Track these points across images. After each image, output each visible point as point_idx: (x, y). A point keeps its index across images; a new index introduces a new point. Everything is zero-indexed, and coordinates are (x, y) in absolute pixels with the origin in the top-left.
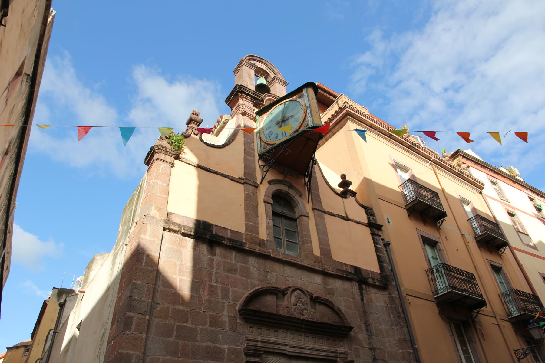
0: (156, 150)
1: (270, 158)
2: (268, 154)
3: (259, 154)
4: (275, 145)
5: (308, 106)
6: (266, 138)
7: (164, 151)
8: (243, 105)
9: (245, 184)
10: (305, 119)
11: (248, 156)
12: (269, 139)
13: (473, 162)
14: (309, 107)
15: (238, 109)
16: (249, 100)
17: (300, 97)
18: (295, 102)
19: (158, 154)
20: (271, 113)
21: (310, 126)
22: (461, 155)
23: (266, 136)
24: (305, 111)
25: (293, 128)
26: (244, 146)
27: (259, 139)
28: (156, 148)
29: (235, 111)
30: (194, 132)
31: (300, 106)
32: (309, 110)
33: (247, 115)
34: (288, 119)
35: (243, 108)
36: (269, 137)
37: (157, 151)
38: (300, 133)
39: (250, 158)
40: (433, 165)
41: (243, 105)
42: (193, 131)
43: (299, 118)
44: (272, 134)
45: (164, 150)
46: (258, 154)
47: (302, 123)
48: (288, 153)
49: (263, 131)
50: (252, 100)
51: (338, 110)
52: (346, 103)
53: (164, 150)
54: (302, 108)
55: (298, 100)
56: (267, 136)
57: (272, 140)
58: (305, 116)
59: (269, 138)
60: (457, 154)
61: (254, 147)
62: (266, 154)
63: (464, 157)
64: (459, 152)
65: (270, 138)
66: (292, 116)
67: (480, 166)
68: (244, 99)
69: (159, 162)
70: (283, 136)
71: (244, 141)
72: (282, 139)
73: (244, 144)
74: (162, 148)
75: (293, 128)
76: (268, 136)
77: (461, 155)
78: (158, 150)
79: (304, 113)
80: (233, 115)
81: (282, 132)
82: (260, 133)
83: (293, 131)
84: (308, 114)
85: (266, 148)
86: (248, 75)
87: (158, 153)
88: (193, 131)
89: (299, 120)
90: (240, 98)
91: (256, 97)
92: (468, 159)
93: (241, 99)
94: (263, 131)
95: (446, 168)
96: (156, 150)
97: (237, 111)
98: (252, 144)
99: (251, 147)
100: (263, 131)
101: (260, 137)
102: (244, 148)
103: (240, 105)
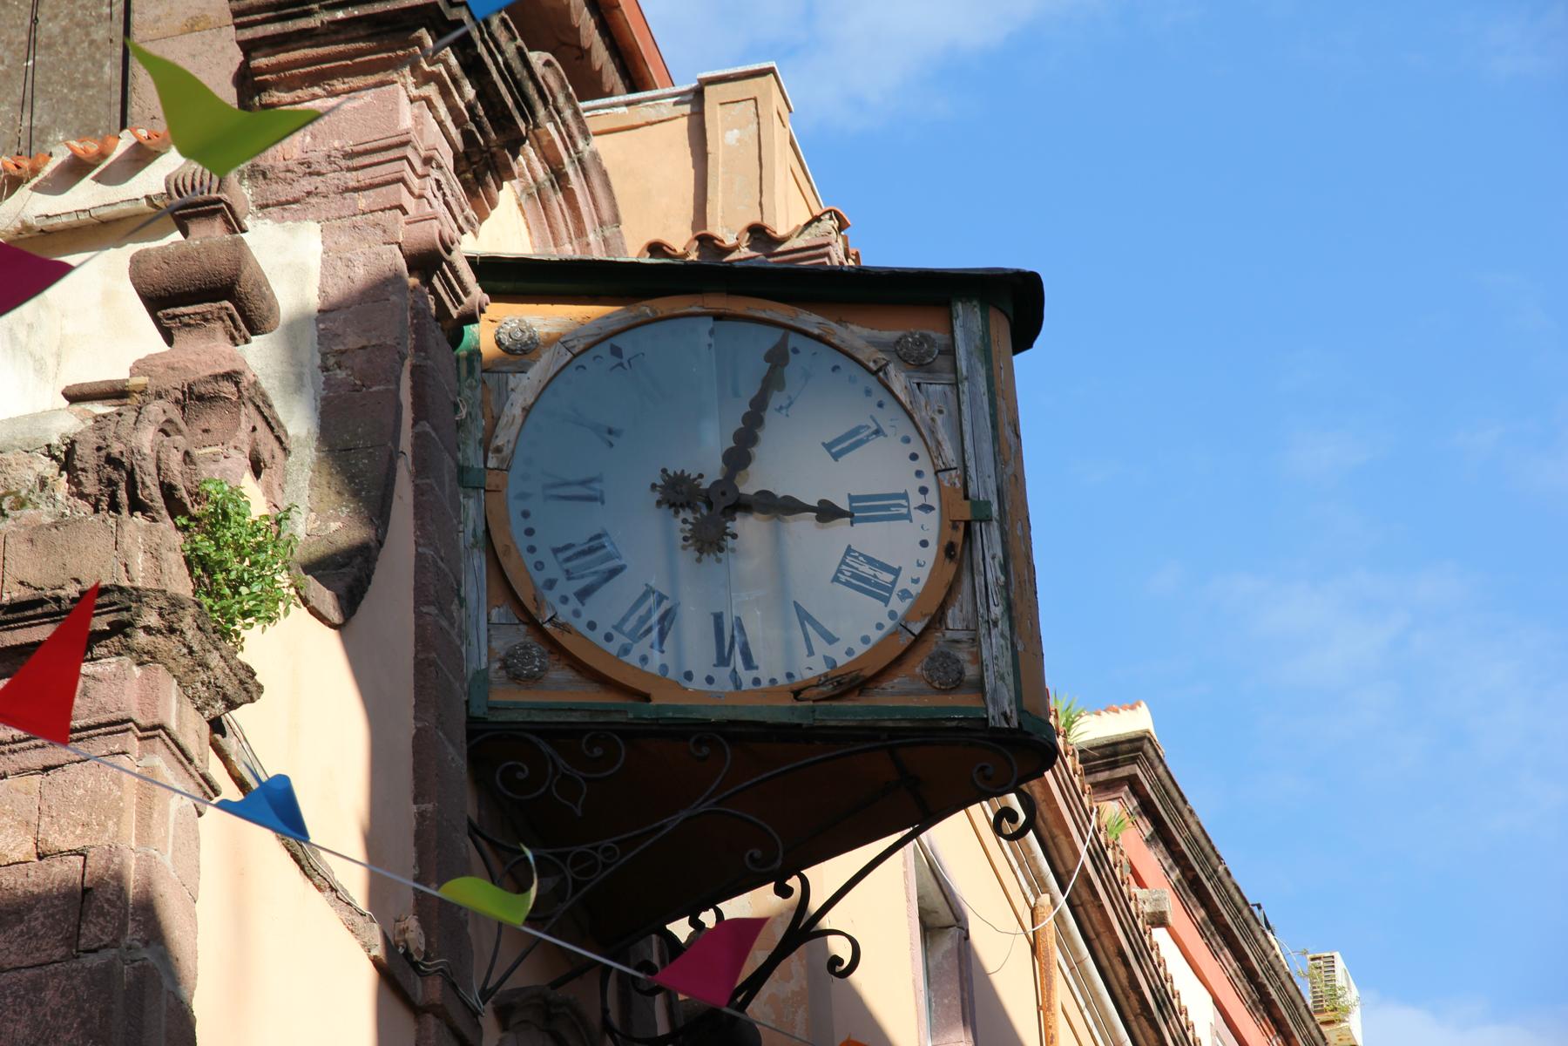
0: (148, 630)
1: (579, 812)
2: (561, 762)
3: (478, 712)
4: (646, 712)
5: (988, 504)
6: (550, 584)
7: (187, 661)
8: (427, 161)
9: (431, 1020)
10: (943, 608)
11: (445, 734)
12: (574, 603)
13: (1176, 874)
14: (995, 524)
15: (364, 176)
16: (453, 109)
17: (918, 361)
18: (868, 392)
19: (140, 664)
20: (616, 352)
21: (997, 722)
22: (1133, 783)
23: (543, 554)
24: (958, 537)
25: (831, 639)
26: (419, 615)
27: (479, 560)
28: (152, 619)
29: (324, 167)
30: (261, 448)
32: (1000, 554)
33: (435, 280)
35: (415, 182)
36: (579, 584)
37: (141, 638)
38: (894, 732)
40: (1045, 898)
41: (427, 161)
42: (254, 429)
43: (896, 572)
44: (614, 572)
45: (196, 648)
47: (919, 639)
48: (757, 853)
50: (474, 116)
51: (729, 241)
52: (829, 224)
53: (191, 652)
55: (899, 380)
56: (553, 569)
58: (952, 589)
59: (583, 594)
60: (1113, 765)
62: (546, 748)
63: (1147, 808)
64: (1133, 760)
65: (591, 601)
66: (827, 512)
67: (1201, 914)
68: (431, 90)
69: (161, 762)
70: (723, 660)
74: (189, 634)
76: (569, 575)
77: (1133, 783)
78: (160, 639)
80: (284, 192)
81: (718, 618)
82: (485, 491)
83: (821, 668)
85: (533, 679)
87: (145, 658)
88: (254, 429)
89: (890, 591)
90: (407, 70)
91: (509, 101)
92: (1162, 835)
93: (410, 80)
95: (1097, 945)
96: (148, 630)
97: (352, 179)
101: (487, 531)
103: (409, 152)
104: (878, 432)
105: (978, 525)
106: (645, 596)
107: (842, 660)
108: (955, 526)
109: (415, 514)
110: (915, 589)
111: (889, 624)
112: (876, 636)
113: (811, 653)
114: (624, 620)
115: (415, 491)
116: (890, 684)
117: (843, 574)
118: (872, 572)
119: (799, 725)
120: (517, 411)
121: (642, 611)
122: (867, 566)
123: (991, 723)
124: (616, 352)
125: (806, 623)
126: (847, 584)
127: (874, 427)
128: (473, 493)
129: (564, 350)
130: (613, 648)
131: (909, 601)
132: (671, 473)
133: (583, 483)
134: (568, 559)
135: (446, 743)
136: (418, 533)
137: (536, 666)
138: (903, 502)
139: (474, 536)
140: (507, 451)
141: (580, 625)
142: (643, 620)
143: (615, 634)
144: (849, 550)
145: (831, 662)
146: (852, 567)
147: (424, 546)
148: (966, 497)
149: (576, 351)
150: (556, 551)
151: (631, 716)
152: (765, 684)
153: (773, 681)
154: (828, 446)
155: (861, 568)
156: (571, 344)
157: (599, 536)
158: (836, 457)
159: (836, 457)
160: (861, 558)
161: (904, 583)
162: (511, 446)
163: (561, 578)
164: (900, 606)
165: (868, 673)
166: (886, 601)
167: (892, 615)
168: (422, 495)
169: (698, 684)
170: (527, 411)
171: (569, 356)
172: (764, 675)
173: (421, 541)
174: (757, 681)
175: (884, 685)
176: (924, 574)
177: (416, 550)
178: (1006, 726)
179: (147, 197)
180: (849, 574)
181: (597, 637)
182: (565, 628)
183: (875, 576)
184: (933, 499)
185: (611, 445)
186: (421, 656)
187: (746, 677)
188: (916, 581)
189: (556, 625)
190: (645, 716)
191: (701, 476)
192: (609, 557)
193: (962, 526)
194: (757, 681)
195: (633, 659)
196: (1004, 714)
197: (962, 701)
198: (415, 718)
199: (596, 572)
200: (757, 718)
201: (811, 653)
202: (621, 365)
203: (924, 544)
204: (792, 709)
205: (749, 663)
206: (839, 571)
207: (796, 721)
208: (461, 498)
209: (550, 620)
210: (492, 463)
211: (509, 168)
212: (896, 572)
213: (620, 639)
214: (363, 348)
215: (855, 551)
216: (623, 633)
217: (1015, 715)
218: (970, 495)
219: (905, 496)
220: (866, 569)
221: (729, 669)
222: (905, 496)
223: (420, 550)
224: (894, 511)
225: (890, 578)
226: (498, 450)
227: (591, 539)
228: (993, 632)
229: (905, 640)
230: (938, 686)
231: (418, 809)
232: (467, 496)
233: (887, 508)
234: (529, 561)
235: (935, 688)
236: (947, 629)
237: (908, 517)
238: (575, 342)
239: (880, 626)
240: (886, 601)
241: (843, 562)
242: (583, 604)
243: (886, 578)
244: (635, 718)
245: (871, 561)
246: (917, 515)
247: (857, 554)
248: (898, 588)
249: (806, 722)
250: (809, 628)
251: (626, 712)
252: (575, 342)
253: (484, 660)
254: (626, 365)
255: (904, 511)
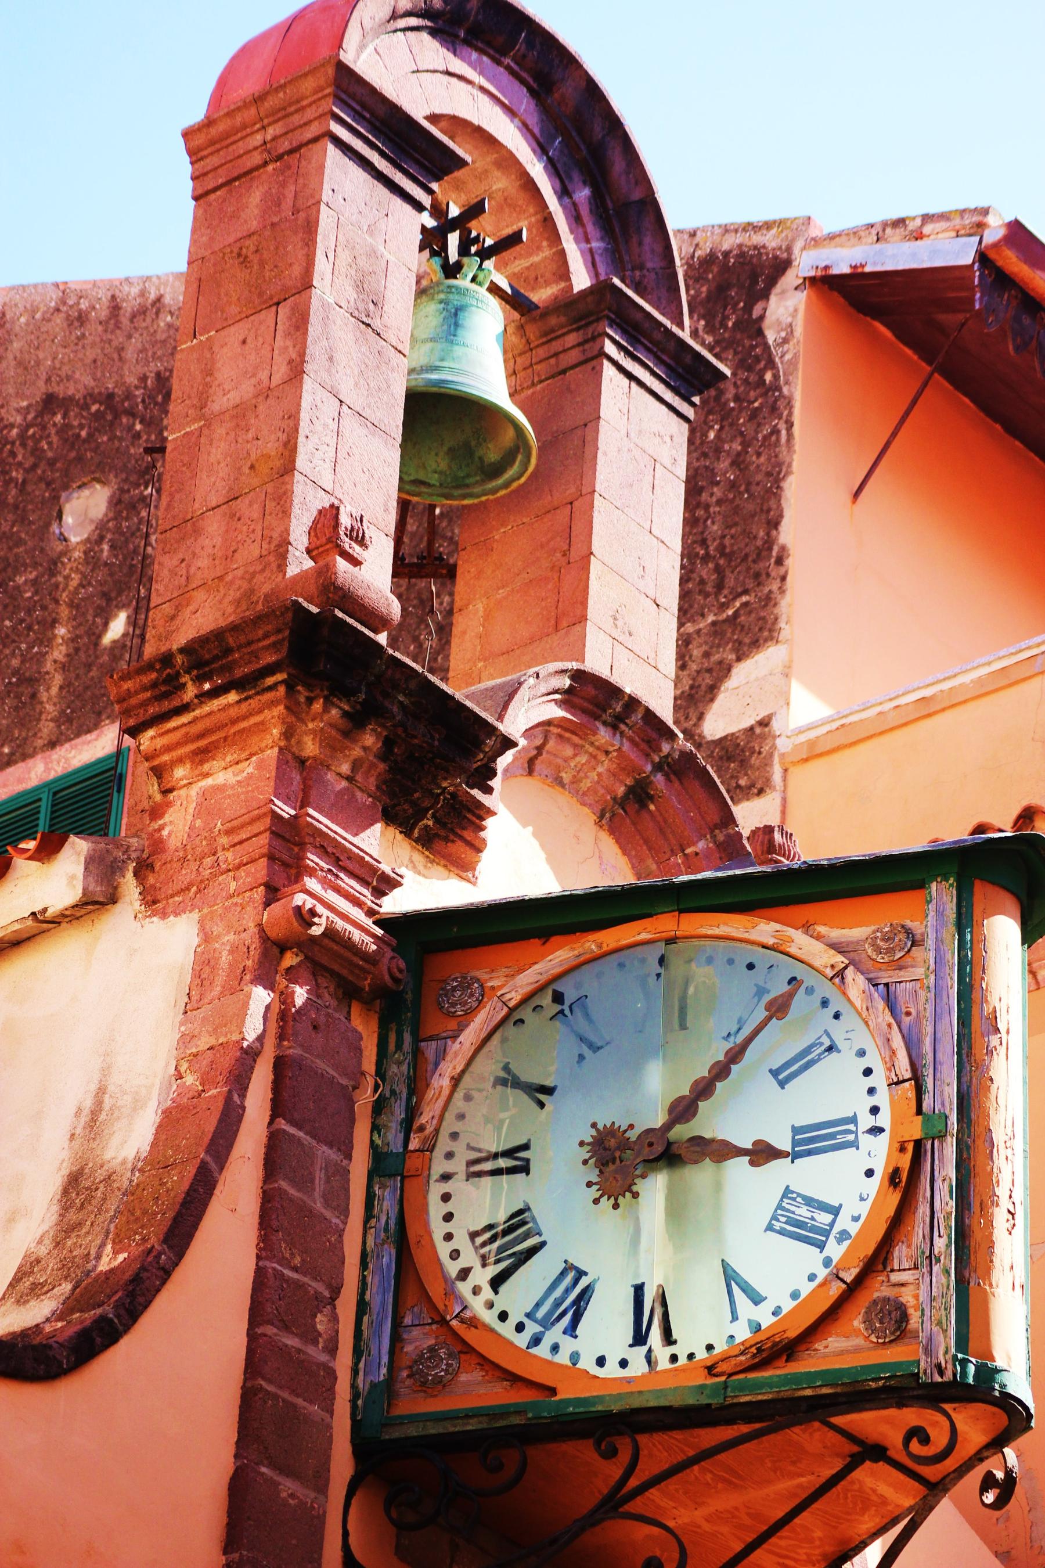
6: (464, 1274)
12: (487, 1292)
20: (558, 998)
23: (461, 1241)
25: (757, 1299)
27: (388, 1257)
31: (868, 1072)
34: (723, 1151)
39: (288, 1486)
43: (835, 1211)
46: (356, 1425)
49: (439, 1166)
54: (875, 1110)
56: (469, 1258)
57: (520, 1328)
59: (496, 1283)
61: (332, 1349)
70: (640, 1338)
71: (260, 1274)
72: (624, 1363)
73: (256, 1314)
75: (757, 1299)
79: (893, 1178)
81: (639, 1290)
82: (403, 1178)
83: (743, 1333)
84: (923, 1209)
86: (360, 286)
89: (827, 1233)
94: (446, 1177)
98: (321, 1322)
99: (311, 1350)
100: (446, 1177)
102: (252, 1366)
104: (830, 1049)
105: (930, 1142)
106: (563, 1274)
107: (767, 1320)
108: (902, 1149)
109: (260, 1224)
110: (854, 1229)
111: (822, 1273)
112: (806, 1289)
113: (735, 1318)
114: (538, 1305)
115: (263, 1199)
116: (824, 1343)
117: (778, 1220)
118: (809, 1215)
119: (709, 1405)
120: (446, 1082)
121: (558, 1293)
122: (805, 1208)
123: (923, 1379)
124: (558, 998)
125: (733, 1283)
126: (782, 1232)
127: (827, 1043)
128: (390, 1182)
129: (500, 1004)
130: (521, 1341)
131: (847, 1243)
132: (600, 1127)
133: (509, 1153)
134: (484, 1244)
135: (278, 1478)
136: (262, 1245)
137: (443, 1370)
138: (852, 1127)
139: (386, 1230)
140: (429, 1129)
141: (489, 1317)
142: (558, 1303)
143: (526, 1321)
144: (787, 1191)
145: (757, 1328)
146: (788, 1211)
147: (267, 1258)
148: (919, 1111)
149: (511, 1004)
150: (473, 1235)
151: (530, 1415)
152: (682, 1360)
153: (691, 1356)
154: (775, 1073)
155: (798, 1211)
156: (508, 996)
157: (520, 1212)
158: (782, 1084)
159: (782, 1084)
160: (799, 1199)
161: (844, 1222)
162: (435, 1122)
163: (477, 1264)
164: (835, 1250)
165: (792, 1334)
166: (821, 1246)
167: (827, 1261)
168: (269, 1202)
169: (611, 1370)
170: (456, 1081)
171: (506, 1009)
172: (681, 1350)
173: (264, 1254)
174: (674, 1358)
175: (816, 1346)
176: (864, 1209)
177: (257, 1265)
178: (940, 1380)
179: (33, 914)
180: (783, 1219)
181: (506, 1330)
182: (474, 1323)
183: (813, 1219)
184: (884, 1119)
185: (542, 1105)
186: (249, 1385)
187: (662, 1354)
188: (855, 1219)
189: (463, 1321)
190: (545, 1414)
191: (631, 1126)
192: (527, 1236)
193: (910, 1147)
194: (674, 1358)
195: (542, 1351)
196: (939, 1366)
197: (897, 1354)
198: (236, 1456)
199: (514, 1254)
200: (663, 1402)
201: (735, 1318)
202: (562, 1012)
203: (869, 1173)
204: (701, 1388)
205: (668, 1338)
206: (774, 1217)
207: (705, 1401)
208: (376, 1189)
209: (456, 1316)
210: (412, 1147)
211: (480, 805)
212: (835, 1211)
213: (532, 1328)
214: (211, 1048)
215: (793, 1192)
216: (536, 1321)
217: (950, 1367)
218: (924, 1109)
219: (853, 1120)
220: (803, 1212)
221: (644, 1349)
222: (853, 1120)
223: (260, 1264)
224: (840, 1139)
225: (831, 1217)
226: (422, 1129)
227: (513, 1216)
228: (935, 1268)
229: (836, 1289)
230: (875, 1340)
231: (227, 1560)
232: (383, 1187)
233: (832, 1136)
234: (443, 1250)
235: (873, 1342)
236: (892, 1271)
237: (854, 1144)
238: (513, 995)
239: (812, 1277)
240: (821, 1246)
241: (779, 1207)
242: (496, 1292)
243: (824, 1218)
244: (534, 1418)
245: (809, 1201)
246: (865, 1140)
247: (795, 1195)
248: (837, 1229)
249: (715, 1401)
250: (735, 1288)
251: (525, 1412)
252: (513, 995)
253: (384, 1371)
254: (567, 1012)
255: (851, 1137)
